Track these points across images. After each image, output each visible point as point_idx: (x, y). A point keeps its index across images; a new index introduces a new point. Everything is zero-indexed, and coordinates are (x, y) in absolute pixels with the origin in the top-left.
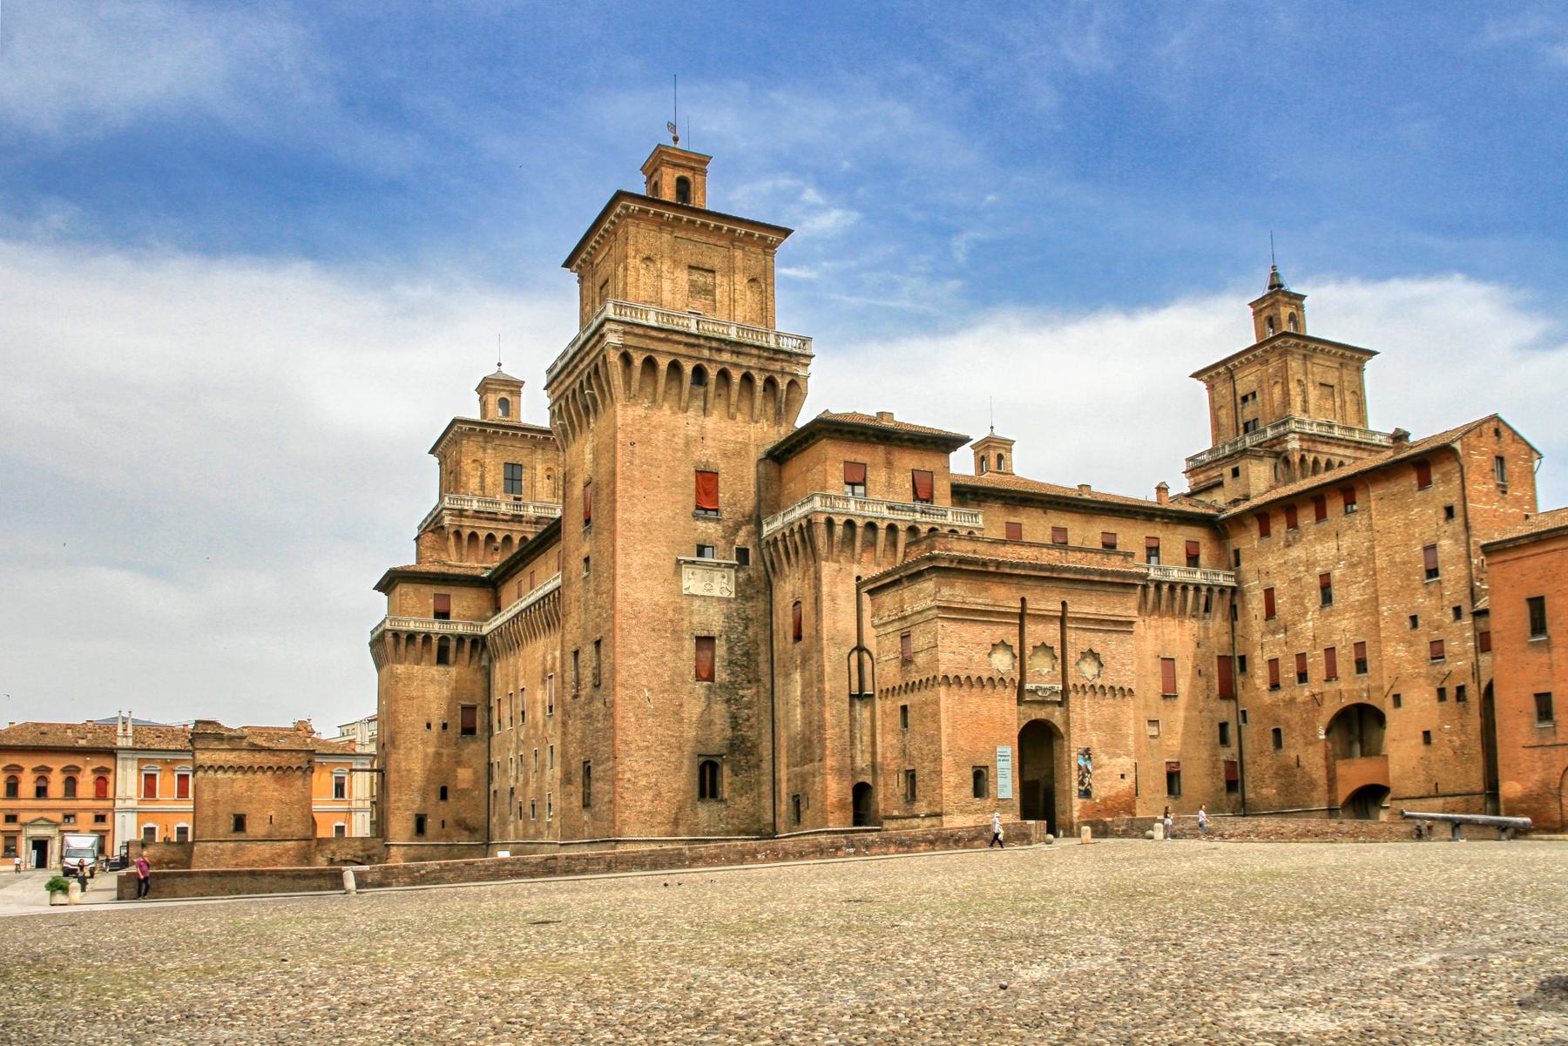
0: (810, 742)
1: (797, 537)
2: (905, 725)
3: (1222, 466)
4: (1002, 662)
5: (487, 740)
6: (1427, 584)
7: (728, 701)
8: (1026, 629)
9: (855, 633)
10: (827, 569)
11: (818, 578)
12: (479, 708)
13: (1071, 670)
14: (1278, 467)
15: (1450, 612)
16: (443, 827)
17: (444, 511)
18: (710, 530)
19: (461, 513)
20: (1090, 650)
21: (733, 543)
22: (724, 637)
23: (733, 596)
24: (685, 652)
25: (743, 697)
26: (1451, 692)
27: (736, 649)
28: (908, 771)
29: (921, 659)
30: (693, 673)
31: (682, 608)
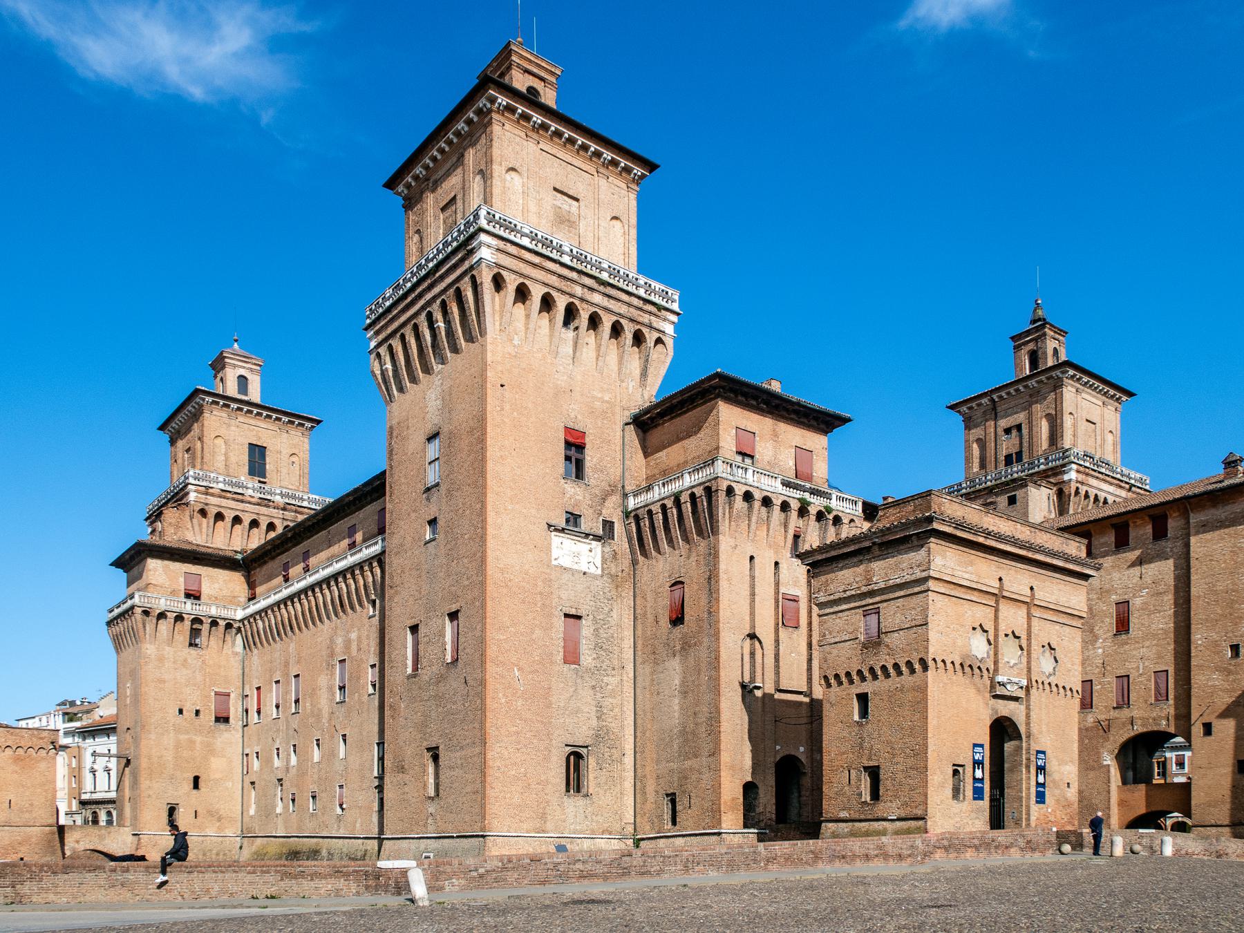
0: (693, 733)
1: (687, 508)
2: (864, 713)
3: (997, 495)
4: (979, 647)
7: (594, 687)
9: (747, 618)
10: (725, 542)
11: (713, 554)
14: (1051, 499)
18: (574, 493)
20: (1049, 644)
22: (591, 616)
23: (599, 572)
24: (554, 630)
27: (601, 631)
29: (894, 640)
30: (562, 654)
31: (550, 580)
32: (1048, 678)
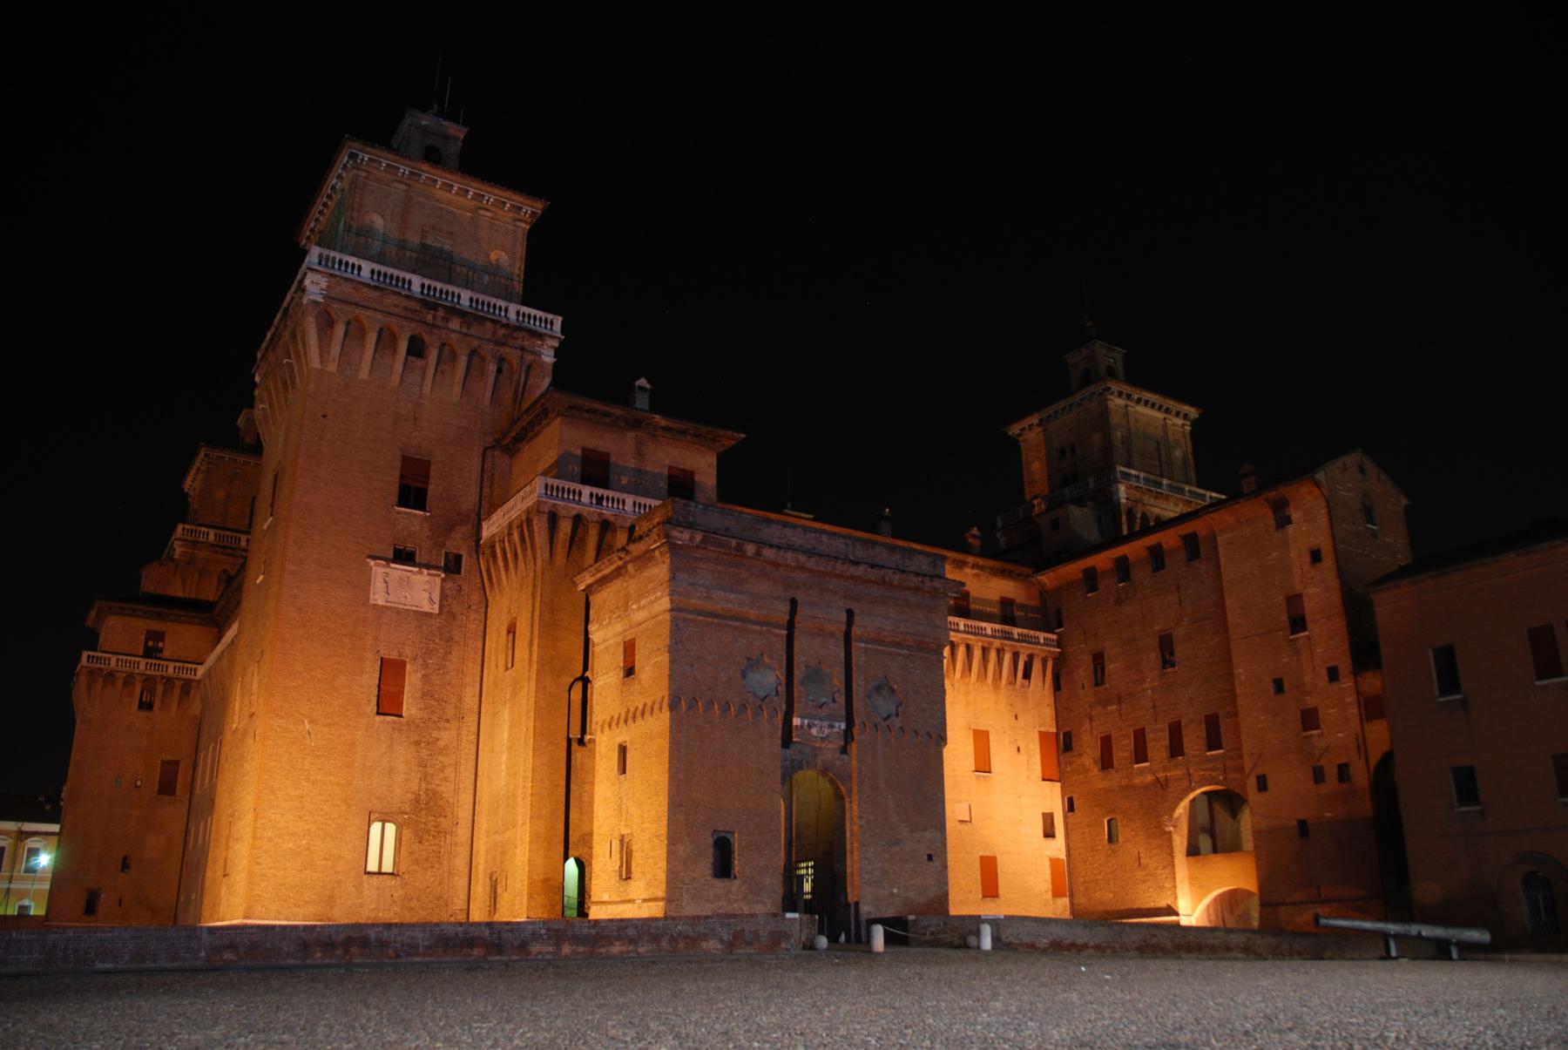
5: (187, 802)
6: (1294, 640)
7: (417, 743)
8: (796, 642)
12: (181, 764)
13: (858, 705)
15: (1324, 672)
16: (120, 905)
17: (176, 542)
19: (195, 544)
21: (444, 545)
23: (436, 609)
25: (438, 740)
26: (1331, 773)
27: (433, 677)
28: (623, 836)
32: (885, 719)
